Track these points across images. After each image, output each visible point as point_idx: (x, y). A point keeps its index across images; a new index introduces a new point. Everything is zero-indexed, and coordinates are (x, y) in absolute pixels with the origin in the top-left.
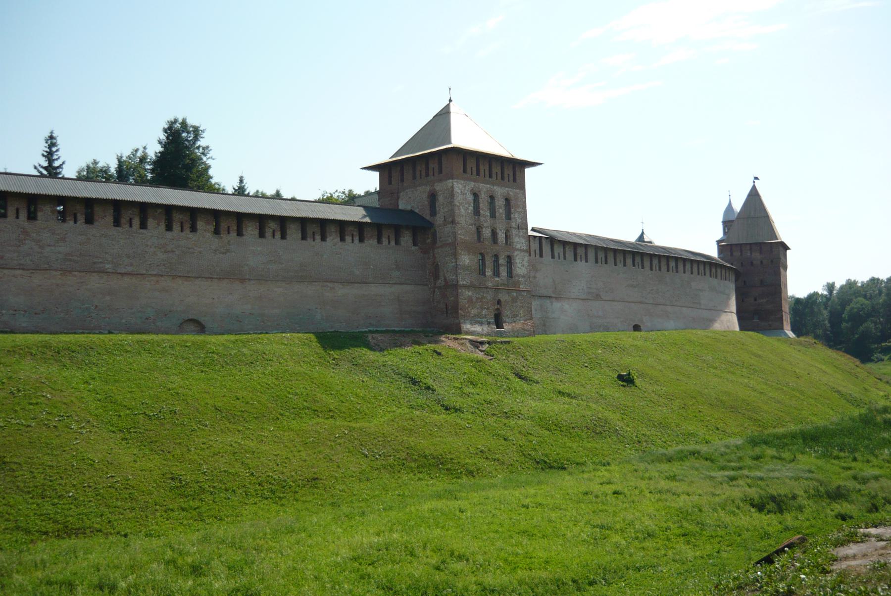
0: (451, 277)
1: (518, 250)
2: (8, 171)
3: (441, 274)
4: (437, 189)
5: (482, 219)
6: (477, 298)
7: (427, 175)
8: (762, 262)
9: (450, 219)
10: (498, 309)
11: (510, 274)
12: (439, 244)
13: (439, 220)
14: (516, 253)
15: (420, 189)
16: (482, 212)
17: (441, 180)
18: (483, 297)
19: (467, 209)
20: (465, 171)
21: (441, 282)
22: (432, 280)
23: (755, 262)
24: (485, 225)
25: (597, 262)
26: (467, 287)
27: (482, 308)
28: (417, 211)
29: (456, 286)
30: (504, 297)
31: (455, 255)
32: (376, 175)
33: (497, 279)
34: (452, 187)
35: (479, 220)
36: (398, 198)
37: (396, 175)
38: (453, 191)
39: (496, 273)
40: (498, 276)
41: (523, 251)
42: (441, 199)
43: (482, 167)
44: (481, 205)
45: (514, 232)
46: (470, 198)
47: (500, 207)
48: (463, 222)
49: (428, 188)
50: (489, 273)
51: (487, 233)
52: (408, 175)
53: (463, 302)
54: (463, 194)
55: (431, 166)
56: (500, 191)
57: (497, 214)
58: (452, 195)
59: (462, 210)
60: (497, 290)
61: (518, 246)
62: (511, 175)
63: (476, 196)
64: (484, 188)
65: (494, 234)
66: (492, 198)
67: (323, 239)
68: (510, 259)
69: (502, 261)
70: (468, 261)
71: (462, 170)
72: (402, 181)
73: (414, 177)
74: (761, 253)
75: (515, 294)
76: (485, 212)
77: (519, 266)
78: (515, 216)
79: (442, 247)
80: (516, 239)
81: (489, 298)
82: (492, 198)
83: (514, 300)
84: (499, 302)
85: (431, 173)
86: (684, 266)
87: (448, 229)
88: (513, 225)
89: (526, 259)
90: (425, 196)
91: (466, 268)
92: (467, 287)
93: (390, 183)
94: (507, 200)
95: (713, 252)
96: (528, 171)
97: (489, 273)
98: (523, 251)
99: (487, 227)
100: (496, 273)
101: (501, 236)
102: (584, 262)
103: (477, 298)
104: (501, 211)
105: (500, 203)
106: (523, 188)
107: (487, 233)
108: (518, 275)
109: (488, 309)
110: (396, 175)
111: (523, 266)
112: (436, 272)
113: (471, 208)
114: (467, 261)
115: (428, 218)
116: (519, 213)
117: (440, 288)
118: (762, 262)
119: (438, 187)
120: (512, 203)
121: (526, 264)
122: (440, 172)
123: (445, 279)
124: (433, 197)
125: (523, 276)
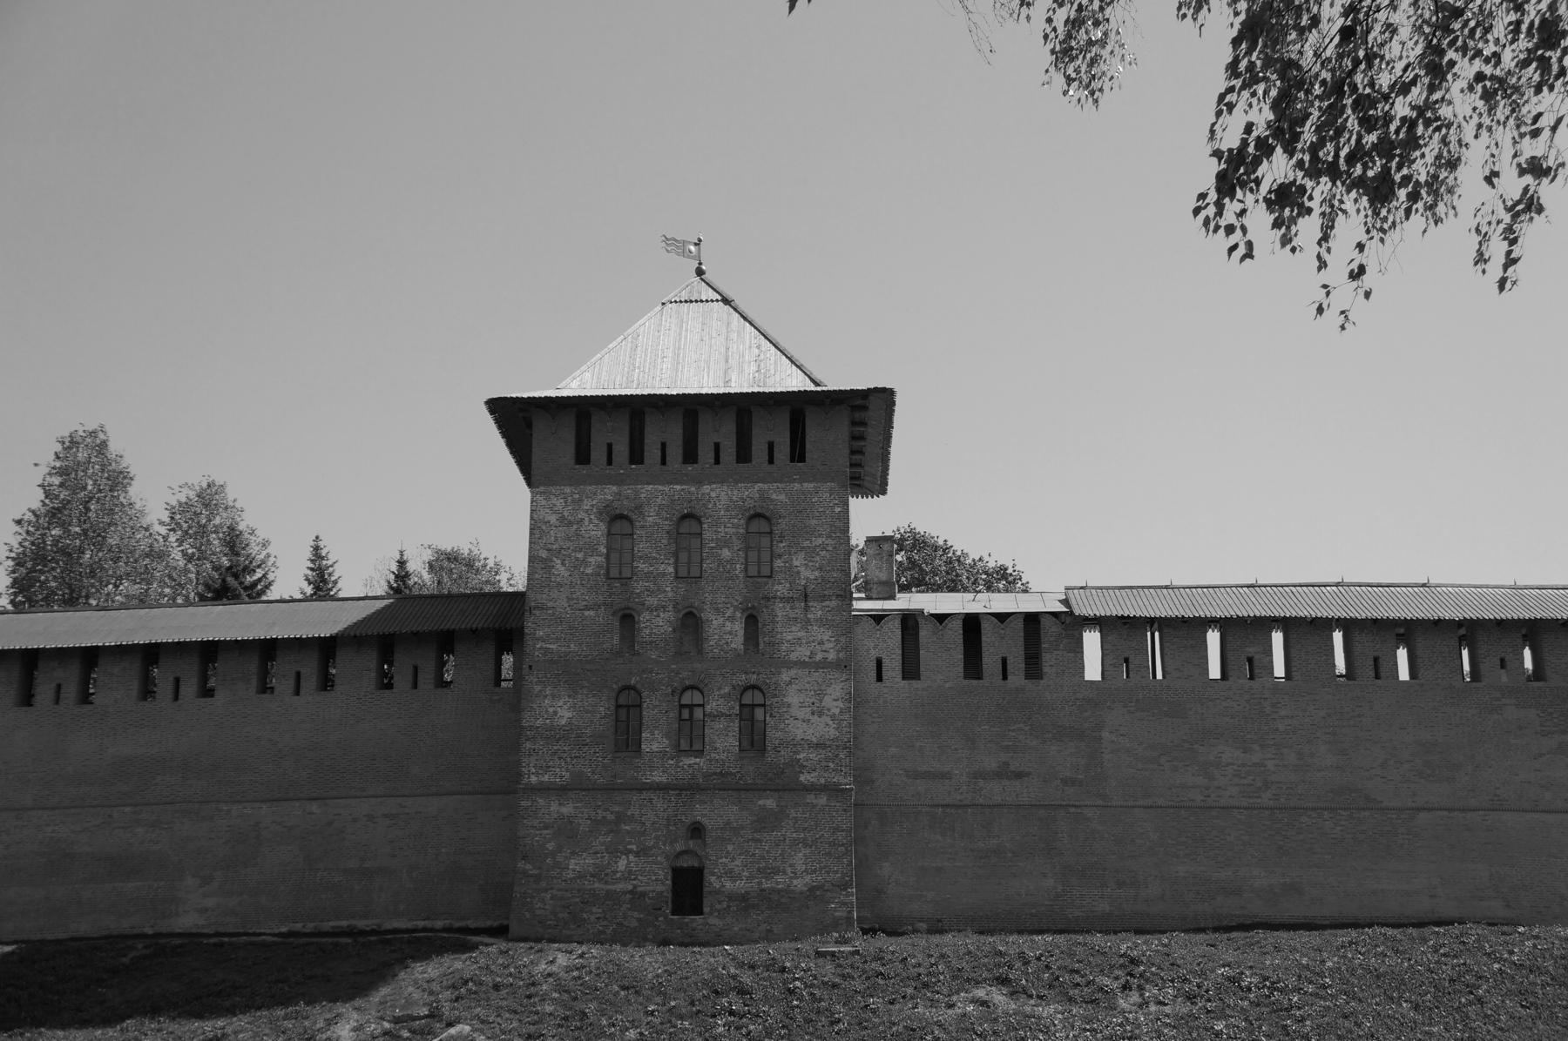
1: (801, 664)
2: (1260, 582)
11: (754, 739)
16: (642, 566)
24: (652, 601)
26: (562, 791)
27: (615, 852)
30: (715, 813)
45: (781, 611)
46: (596, 530)
51: (657, 624)
60: (688, 789)
61: (802, 653)
65: (691, 622)
80: (790, 634)
82: (689, 519)
83: (766, 821)
84: (697, 831)
88: (781, 589)
92: (562, 791)
97: (654, 742)
104: (726, 553)
107: (657, 624)
114: (565, 714)
125: (819, 746)
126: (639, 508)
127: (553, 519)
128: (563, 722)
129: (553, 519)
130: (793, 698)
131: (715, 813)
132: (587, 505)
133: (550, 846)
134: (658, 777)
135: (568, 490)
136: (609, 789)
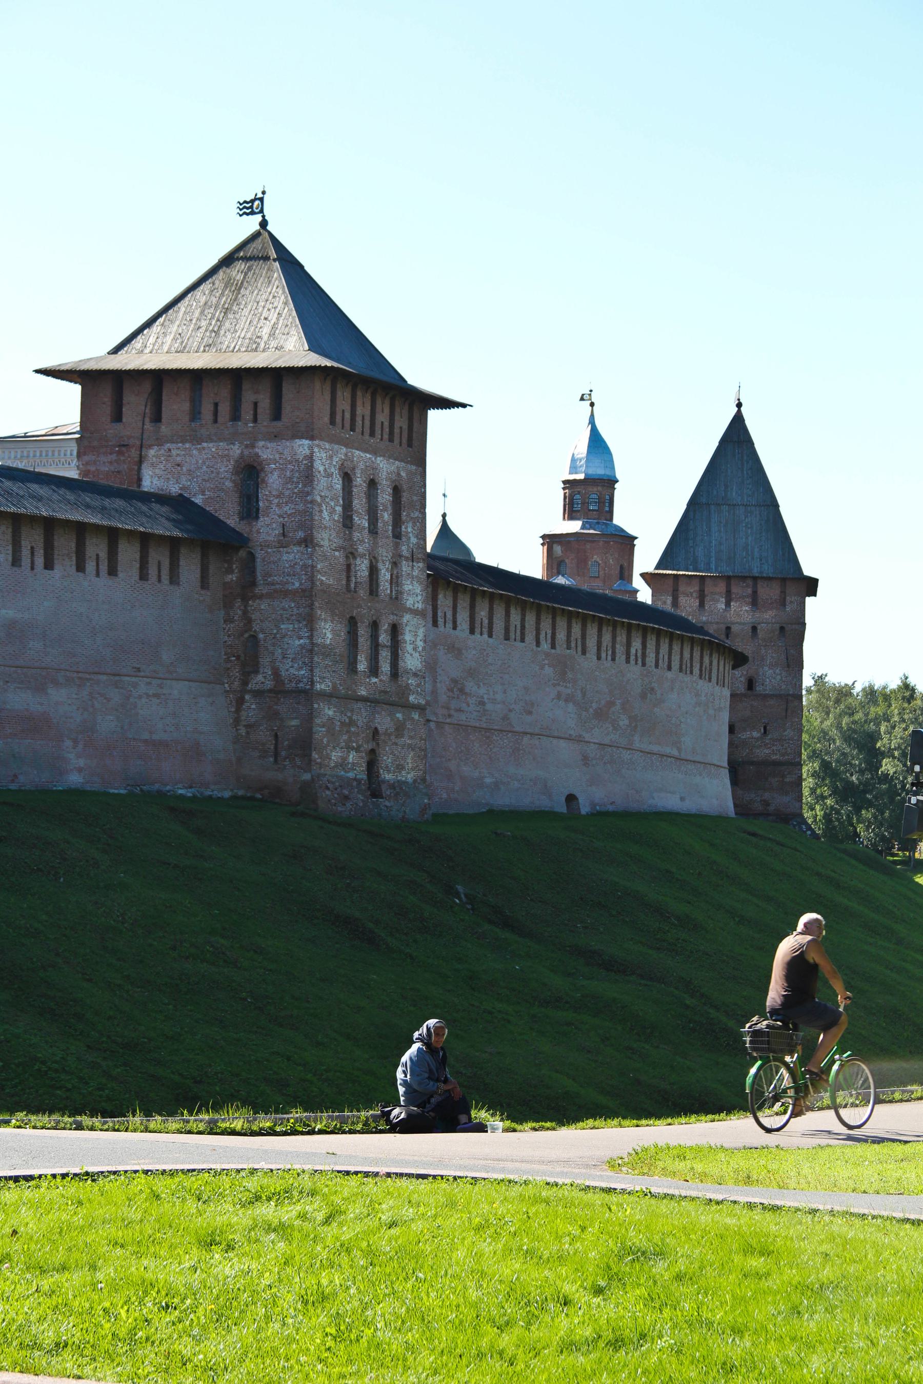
0: (292, 670)
3: (265, 661)
4: (265, 455)
5: (356, 535)
6: (343, 724)
7: (236, 416)
8: (754, 629)
9: (301, 534)
10: (373, 751)
12: (261, 589)
13: (266, 529)
14: (407, 617)
15: (212, 447)
17: (276, 437)
18: (352, 723)
19: (333, 511)
20: (333, 422)
21: (262, 680)
22: (236, 672)
23: (735, 629)
24: (361, 549)
25: (507, 638)
27: (349, 748)
28: (198, 500)
29: (306, 695)
30: (384, 722)
31: (310, 621)
32: (74, 391)
33: (374, 680)
34: (310, 458)
35: (351, 539)
36: (140, 461)
37: (136, 403)
38: (310, 467)
39: (374, 670)
40: (376, 676)
41: (415, 612)
42: (273, 481)
43: (359, 411)
44: (355, 502)
45: (405, 567)
47: (385, 510)
48: (326, 543)
49: (236, 450)
50: (362, 666)
52: (176, 405)
53: (320, 733)
54: (329, 475)
55: (248, 397)
56: (386, 468)
57: (380, 525)
58: (308, 475)
59: (325, 514)
62: (405, 427)
63: (347, 478)
64: (361, 458)
65: (373, 571)
66: (372, 484)
67: (49, 565)
68: (395, 630)
69: (384, 638)
70: (329, 635)
71: (327, 419)
72: (157, 418)
73: (195, 414)
74: (754, 602)
75: (399, 715)
76: (361, 521)
77: (409, 648)
78: (408, 528)
79: (269, 596)
81: (360, 723)
82: (372, 484)
83: (400, 729)
85: (247, 412)
86: (472, 607)
87: (292, 555)
89: (421, 632)
90: (225, 469)
91: (327, 651)
93: (118, 417)
94: (397, 491)
95: (530, 563)
96: (434, 415)
97: (362, 666)
98: (415, 612)
99: (362, 556)
100: (374, 670)
101: (385, 575)
102: (485, 636)
103: (343, 724)
105: (385, 497)
106: (420, 461)
107: (362, 568)
108: (407, 672)
109: (357, 750)
110: (136, 403)
111: (415, 649)
112: (249, 654)
113: (339, 509)
115: (232, 521)
116: (414, 521)
117: (258, 694)
118: (754, 629)
119: (266, 451)
120: (405, 497)
121: (420, 644)
122: (277, 415)
123: (276, 673)
124: (250, 473)
125: (415, 675)
126: (354, 469)
127: (321, 469)
128: (328, 642)
129: (321, 469)
130: (408, 637)
131: (384, 722)
132: (335, 459)
133: (325, 740)
134: (363, 692)
135: (327, 446)
136: (347, 698)
